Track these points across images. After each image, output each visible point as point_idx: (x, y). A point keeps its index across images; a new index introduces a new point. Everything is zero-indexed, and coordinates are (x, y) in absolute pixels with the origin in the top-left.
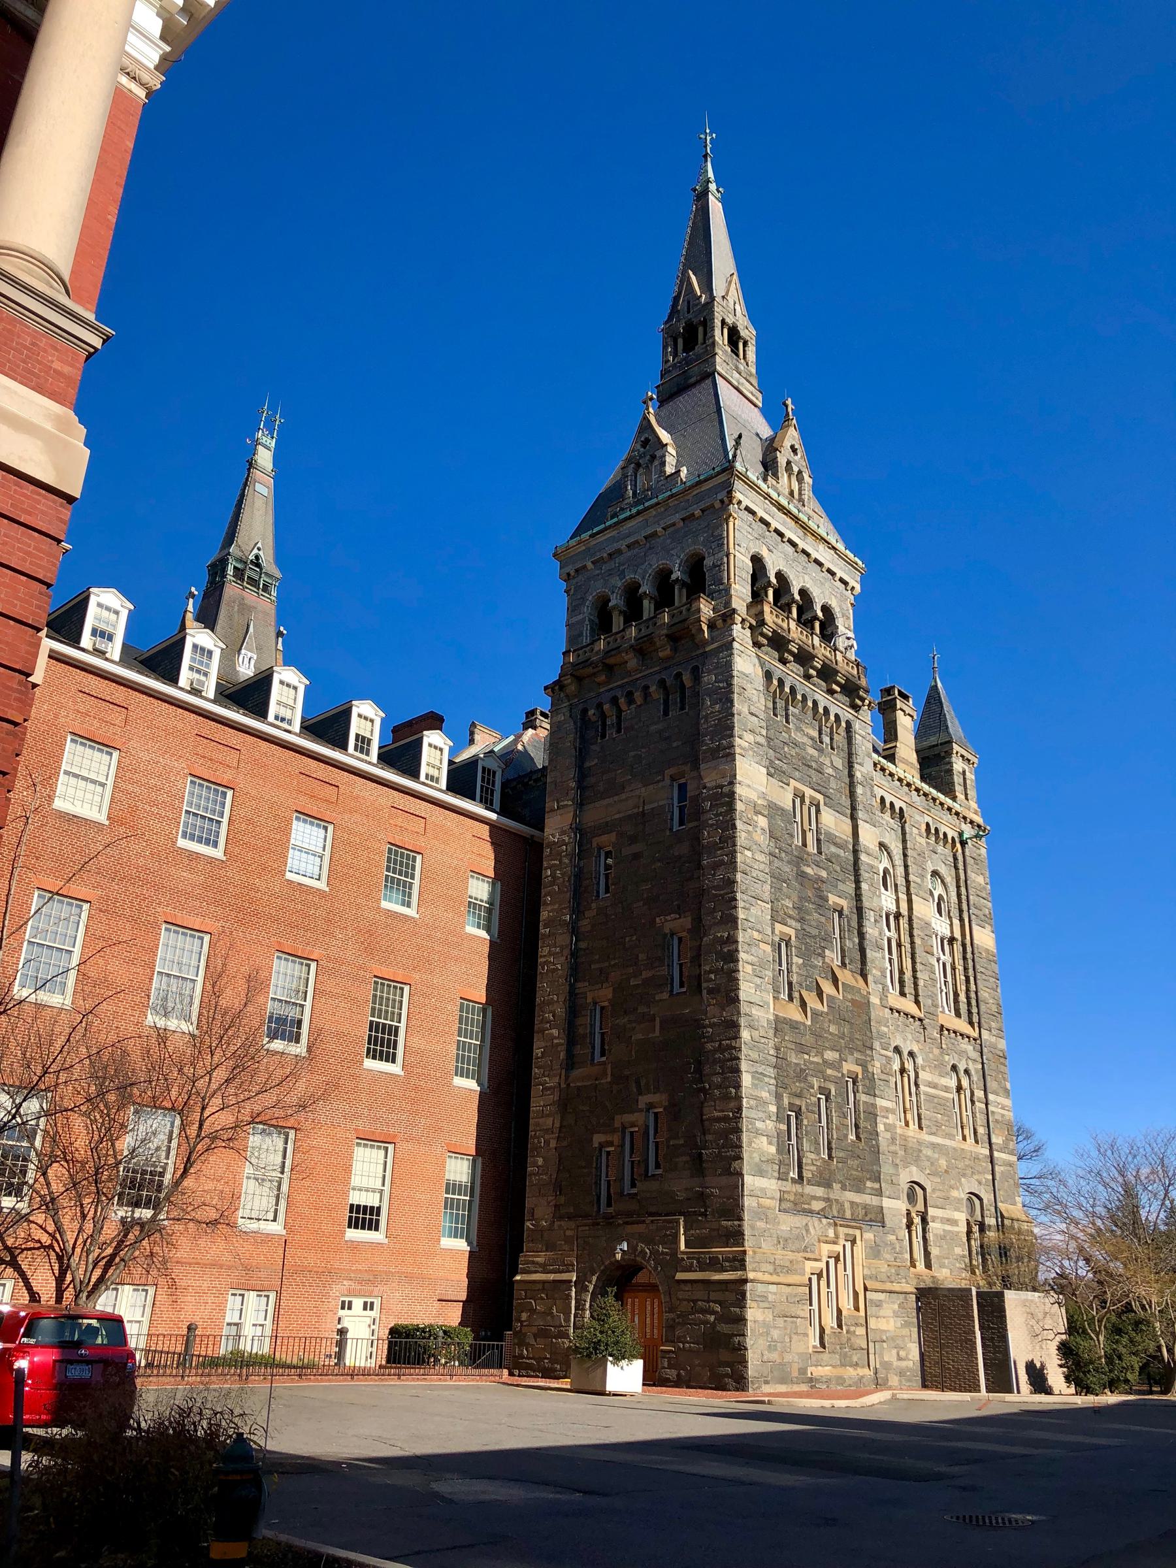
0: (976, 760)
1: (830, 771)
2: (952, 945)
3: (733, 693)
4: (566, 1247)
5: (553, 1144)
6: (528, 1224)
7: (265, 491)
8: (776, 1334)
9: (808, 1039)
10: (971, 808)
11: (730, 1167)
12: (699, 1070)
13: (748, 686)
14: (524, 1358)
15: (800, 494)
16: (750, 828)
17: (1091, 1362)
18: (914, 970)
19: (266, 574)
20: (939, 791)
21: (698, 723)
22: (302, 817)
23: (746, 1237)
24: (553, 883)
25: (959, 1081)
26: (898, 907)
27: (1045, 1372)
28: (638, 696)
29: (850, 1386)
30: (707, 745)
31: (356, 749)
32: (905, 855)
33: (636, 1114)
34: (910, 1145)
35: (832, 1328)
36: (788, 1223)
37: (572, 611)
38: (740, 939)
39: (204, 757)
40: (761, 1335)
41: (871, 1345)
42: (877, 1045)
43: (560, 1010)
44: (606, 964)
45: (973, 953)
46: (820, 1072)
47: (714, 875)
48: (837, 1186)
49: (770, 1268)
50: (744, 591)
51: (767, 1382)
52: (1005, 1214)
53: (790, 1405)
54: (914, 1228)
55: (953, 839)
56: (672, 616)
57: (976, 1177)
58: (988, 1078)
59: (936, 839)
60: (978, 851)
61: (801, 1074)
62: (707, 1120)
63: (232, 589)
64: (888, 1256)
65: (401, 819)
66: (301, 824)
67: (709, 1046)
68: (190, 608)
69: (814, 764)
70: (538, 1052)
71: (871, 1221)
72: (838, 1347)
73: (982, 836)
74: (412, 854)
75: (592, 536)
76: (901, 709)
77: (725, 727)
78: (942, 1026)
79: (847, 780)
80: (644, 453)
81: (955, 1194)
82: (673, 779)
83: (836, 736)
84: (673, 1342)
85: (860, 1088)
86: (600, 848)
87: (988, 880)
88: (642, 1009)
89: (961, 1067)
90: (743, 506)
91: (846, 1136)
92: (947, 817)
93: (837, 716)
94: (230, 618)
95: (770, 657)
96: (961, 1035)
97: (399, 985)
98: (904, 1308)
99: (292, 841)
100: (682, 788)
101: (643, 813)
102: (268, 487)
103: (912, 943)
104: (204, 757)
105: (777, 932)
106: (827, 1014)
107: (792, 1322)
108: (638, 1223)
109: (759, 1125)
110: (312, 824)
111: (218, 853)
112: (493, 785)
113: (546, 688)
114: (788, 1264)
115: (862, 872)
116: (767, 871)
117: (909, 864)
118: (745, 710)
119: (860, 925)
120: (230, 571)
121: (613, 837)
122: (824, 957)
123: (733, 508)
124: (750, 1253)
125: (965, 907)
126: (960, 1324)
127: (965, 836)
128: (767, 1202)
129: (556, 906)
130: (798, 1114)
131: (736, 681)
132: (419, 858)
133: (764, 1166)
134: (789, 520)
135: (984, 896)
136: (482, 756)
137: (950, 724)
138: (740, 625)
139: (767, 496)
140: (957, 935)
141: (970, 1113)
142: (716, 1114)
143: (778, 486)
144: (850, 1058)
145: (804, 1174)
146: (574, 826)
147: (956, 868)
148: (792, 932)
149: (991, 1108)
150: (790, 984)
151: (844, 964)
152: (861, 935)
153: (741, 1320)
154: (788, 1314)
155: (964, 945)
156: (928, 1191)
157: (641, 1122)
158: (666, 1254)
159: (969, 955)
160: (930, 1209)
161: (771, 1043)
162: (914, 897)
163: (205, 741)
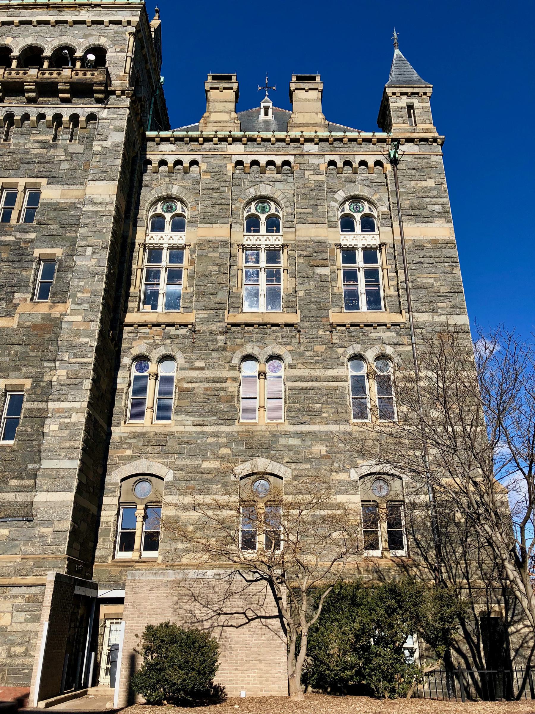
76: (297, 89)
134: (40, 10)
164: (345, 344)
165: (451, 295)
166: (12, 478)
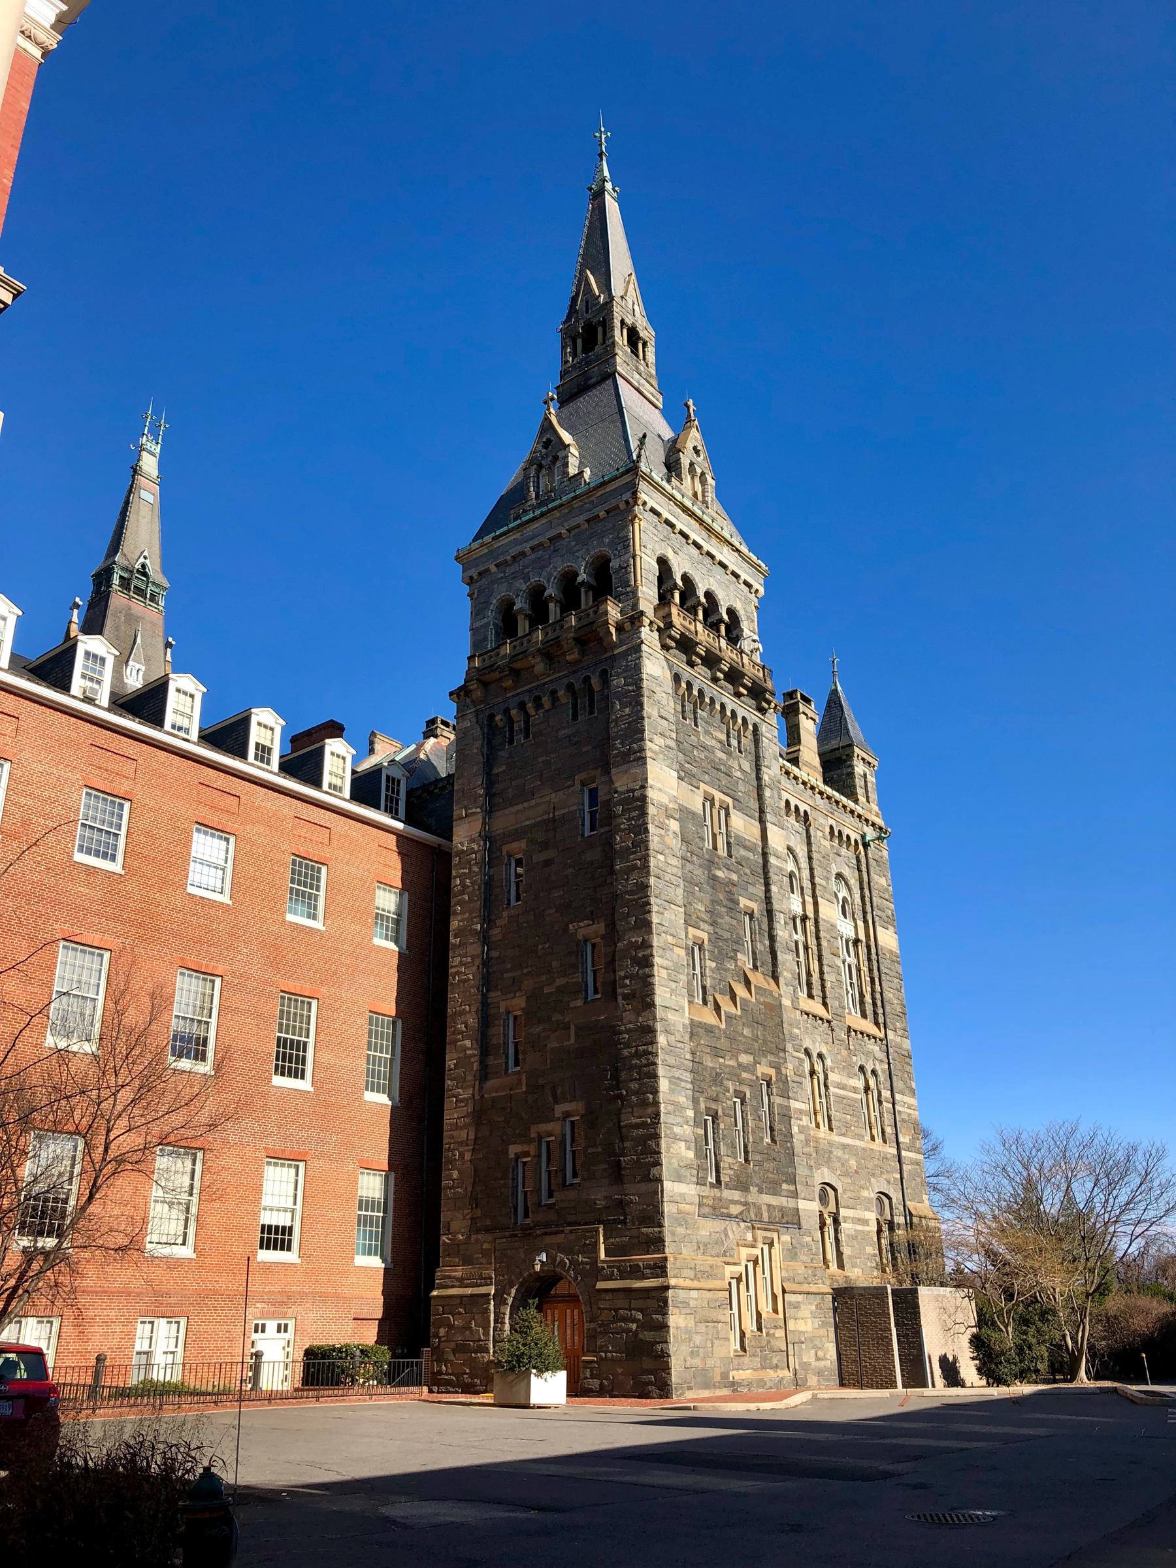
0: (876, 763)
1: (738, 774)
2: (857, 946)
3: (643, 696)
4: (484, 1261)
5: (468, 1156)
6: (444, 1238)
7: (150, 498)
8: (698, 1339)
9: (723, 1043)
10: (872, 809)
11: (650, 1173)
12: (616, 1077)
13: (657, 689)
14: (442, 1374)
15: (704, 496)
16: (663, 832)
17: (1003, 1353)
18: (822, 973)
19: (153, 583)
20: (842, 793)
21: (608, 728)
22: (203, 828)
23: (667, 1244)
24: (462, 892)
25: (867, 1081)
26: (804, 909)
27: (958, 1365)
28: (546, 701)
29: (771, 1388)
30: (617, 749)
31: (256, 759)
32: (810, 858)
33: (552, 1123)
34: (821, 1146)
35: (752, 1331)
36: (708, 1228)
37: (477, 615)
38: (655, 944)
39: (100, 768)
40: (683, 1341)
41: (790, 1347)
42: (789, 1047)
43: (472, 1021)
44: (519, 973)
45: (877, 954)
46: (735, 1075)
47: (627, 880)
48: (753, 1189)
49: (691, 1274)
50: (651, 593)
51: (690, 1388)
52: (914, 1212)
53: (716, 1410)
54: (826, 1229)
55: (856, 841)
56: (579, 619)
57: (885, 1176)
58: (894, 1078)
59: (840, 842)
60: (880, 853)
61: (717, 1079)
62: (626, 1126)
63: (118, 600)
64: (804, 1258)
65: (304, 830)
66: (202, 836)
67: (625, 1052)
68: (75, 619)
69: (722, 767)
70: (450, 1063)
71: (787, 1223)
72: (758, 1350)
73: (884, 838)
74: (317, 865)
75: (494, 539)
77: (636, 730)
78: (849, 1027)
79: (755, 783)
80: (546, 454)
81: (865, 1193)
82: (583, 784)
83: (743, 739)
84: (594, 1351)
85: (774, 1091)
86: (510, 856)
87: (890, 882)
88: (556, 1017)
89: (869, 1068)
90: (648, 507)
91: (762, 1139)
92: (849, 820)
93: (744, 719)
94: (117, 629)
95: (678, 659)
96: (868, 1036)
97: (306, 1000)
98: (821, 1309)
99: (193, 854)
100: (593, 794)
101: (554, 820)
102: (153, 494)
103: (819, 945)
104: (100, 768)
105: (690, 936)
106: (741, 1017)
107: (714, 1327)
108: (556, 1233)
109: (677, 1130)
110: (213, 835)
111: (116, 867)
112: (398, 794)
113: (451, 694)
114: (708, 1269)
115: (771, 874)
116: (679, 875)
117: (815, 866)
118: (655, 714)
119: (771, 928)
120: (116, 580)
121: (523, 844)
122: (736, 960)
123: (638, 509)
124: (671, 1259)
125: (869, 909)
126: (876, 1322)
127: (868, 838)
128: (686, 1208)
129: (467, 915)
130: (715, 1118)
131: (645, 684)
132: (324, 869)
133: (683, 1172)
134: (693, 522)
135: (887, 897)
136: (386, 764)
137: (850, 727)
138: (648, 628)
139: (671, 498)
140: (862, 937)
141: (877, 1113)
142: (634, 1120)
143: (682, 487)
144: (764, 1060)
145: (722, 1179)
146: (483, 833)
147: (860, 870)
148: (705, 936)
149: (898, 1108)
150: (704, 988)
151: (755, 967)
152: (772, 938)
153: (664, 1327)
154: (710, 1319)
155: (868, 947)
156: (840, 1191)
157: (557, 1131)
158: (587, 1263)
159: (874, 957)
160: (841, 1210)
161: (687, 1048)
162: (820, 899)
163: (100, 750)
164: (857, 1053)
165: (901, 1015)
166: (783, 1181)
